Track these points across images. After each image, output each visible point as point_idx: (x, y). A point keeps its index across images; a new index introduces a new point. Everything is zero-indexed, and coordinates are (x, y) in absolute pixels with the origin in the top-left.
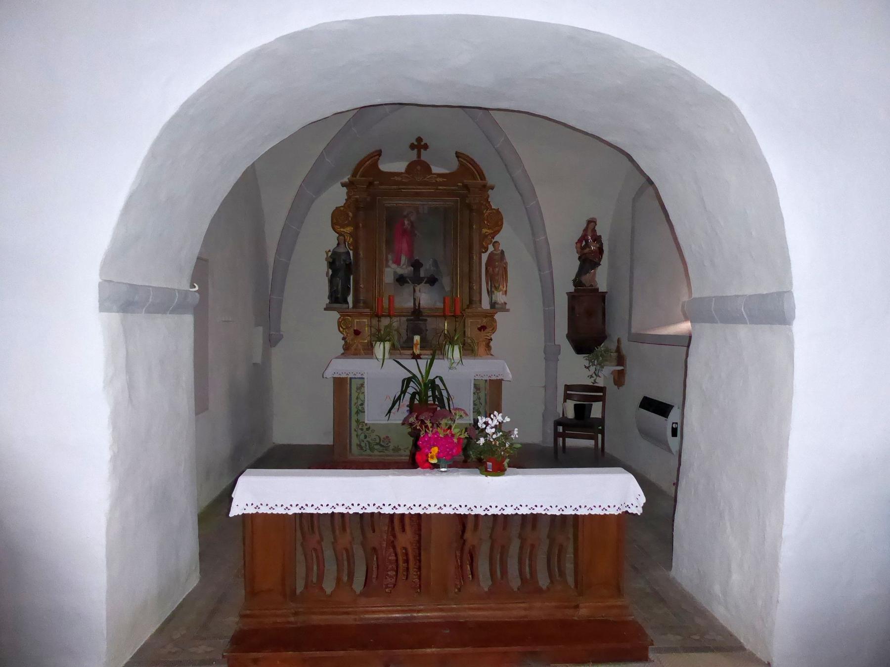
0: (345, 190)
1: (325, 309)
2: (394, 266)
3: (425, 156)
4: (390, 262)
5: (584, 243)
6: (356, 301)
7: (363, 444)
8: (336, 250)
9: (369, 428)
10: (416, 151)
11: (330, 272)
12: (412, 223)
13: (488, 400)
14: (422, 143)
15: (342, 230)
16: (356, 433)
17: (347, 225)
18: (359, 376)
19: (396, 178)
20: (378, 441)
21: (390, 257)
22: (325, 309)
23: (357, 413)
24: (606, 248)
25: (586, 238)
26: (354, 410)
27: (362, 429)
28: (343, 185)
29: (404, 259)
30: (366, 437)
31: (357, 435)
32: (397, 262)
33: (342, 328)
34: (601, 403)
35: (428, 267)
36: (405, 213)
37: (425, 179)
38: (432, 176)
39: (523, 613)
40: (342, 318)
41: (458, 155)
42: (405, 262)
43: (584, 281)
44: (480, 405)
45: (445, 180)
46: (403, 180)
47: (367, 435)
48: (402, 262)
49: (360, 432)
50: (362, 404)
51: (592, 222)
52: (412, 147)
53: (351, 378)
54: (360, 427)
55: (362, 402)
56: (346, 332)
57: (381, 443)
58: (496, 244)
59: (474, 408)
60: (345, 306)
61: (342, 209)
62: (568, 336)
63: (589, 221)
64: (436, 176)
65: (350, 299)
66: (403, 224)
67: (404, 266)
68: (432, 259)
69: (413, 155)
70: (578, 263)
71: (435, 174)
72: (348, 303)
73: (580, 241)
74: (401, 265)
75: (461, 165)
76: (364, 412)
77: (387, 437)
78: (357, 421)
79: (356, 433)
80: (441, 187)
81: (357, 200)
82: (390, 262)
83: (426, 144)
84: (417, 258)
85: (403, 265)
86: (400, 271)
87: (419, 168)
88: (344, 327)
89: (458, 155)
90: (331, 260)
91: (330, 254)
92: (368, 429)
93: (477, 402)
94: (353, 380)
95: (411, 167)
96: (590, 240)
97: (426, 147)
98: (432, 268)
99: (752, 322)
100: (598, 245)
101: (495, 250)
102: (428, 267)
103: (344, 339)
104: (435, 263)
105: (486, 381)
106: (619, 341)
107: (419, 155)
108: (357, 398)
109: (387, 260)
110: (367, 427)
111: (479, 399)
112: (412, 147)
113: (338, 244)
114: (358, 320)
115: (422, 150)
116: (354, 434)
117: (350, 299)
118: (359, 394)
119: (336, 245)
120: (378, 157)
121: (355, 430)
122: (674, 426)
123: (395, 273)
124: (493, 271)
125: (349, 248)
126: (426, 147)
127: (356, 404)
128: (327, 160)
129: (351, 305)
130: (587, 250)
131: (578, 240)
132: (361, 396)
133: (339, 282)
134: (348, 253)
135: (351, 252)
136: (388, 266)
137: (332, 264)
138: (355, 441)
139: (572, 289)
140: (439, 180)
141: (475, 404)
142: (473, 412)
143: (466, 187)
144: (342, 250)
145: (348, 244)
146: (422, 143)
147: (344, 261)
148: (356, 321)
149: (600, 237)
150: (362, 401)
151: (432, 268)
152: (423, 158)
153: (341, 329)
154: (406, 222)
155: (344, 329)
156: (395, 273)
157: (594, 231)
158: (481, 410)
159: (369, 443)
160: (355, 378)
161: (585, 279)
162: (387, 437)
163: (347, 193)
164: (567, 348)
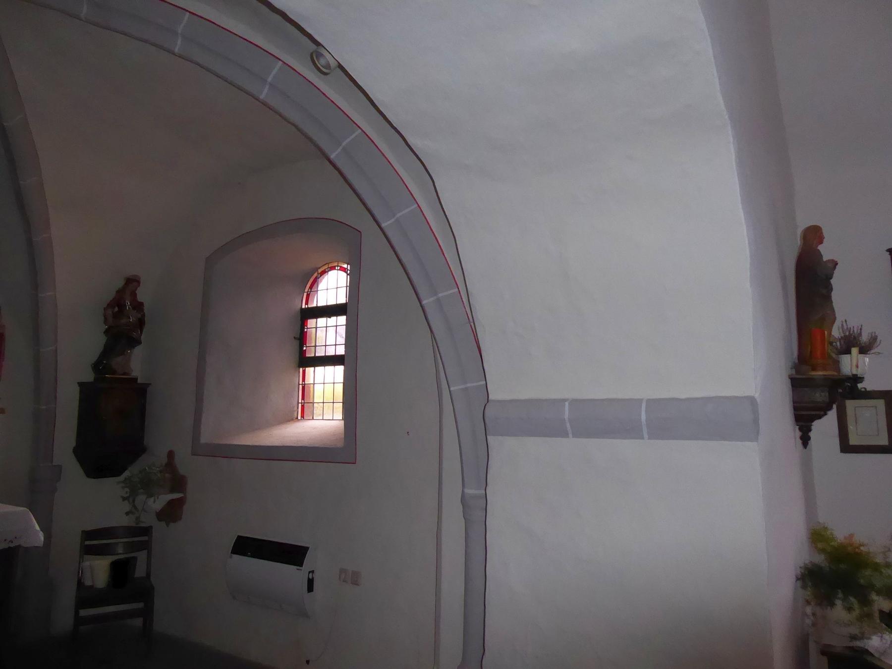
34: (145, 552)
51: (132, 282)
62: (77, 451)
70: (103, 339)
73: (110, 305)
99: (575, 435)
100: (139, 316)
106: (171, 455)
122: (311, 577)
130: (124, 321)
131: (108, 305)
149: (141, 304)
157: (134, 295)
161: (117, 362)
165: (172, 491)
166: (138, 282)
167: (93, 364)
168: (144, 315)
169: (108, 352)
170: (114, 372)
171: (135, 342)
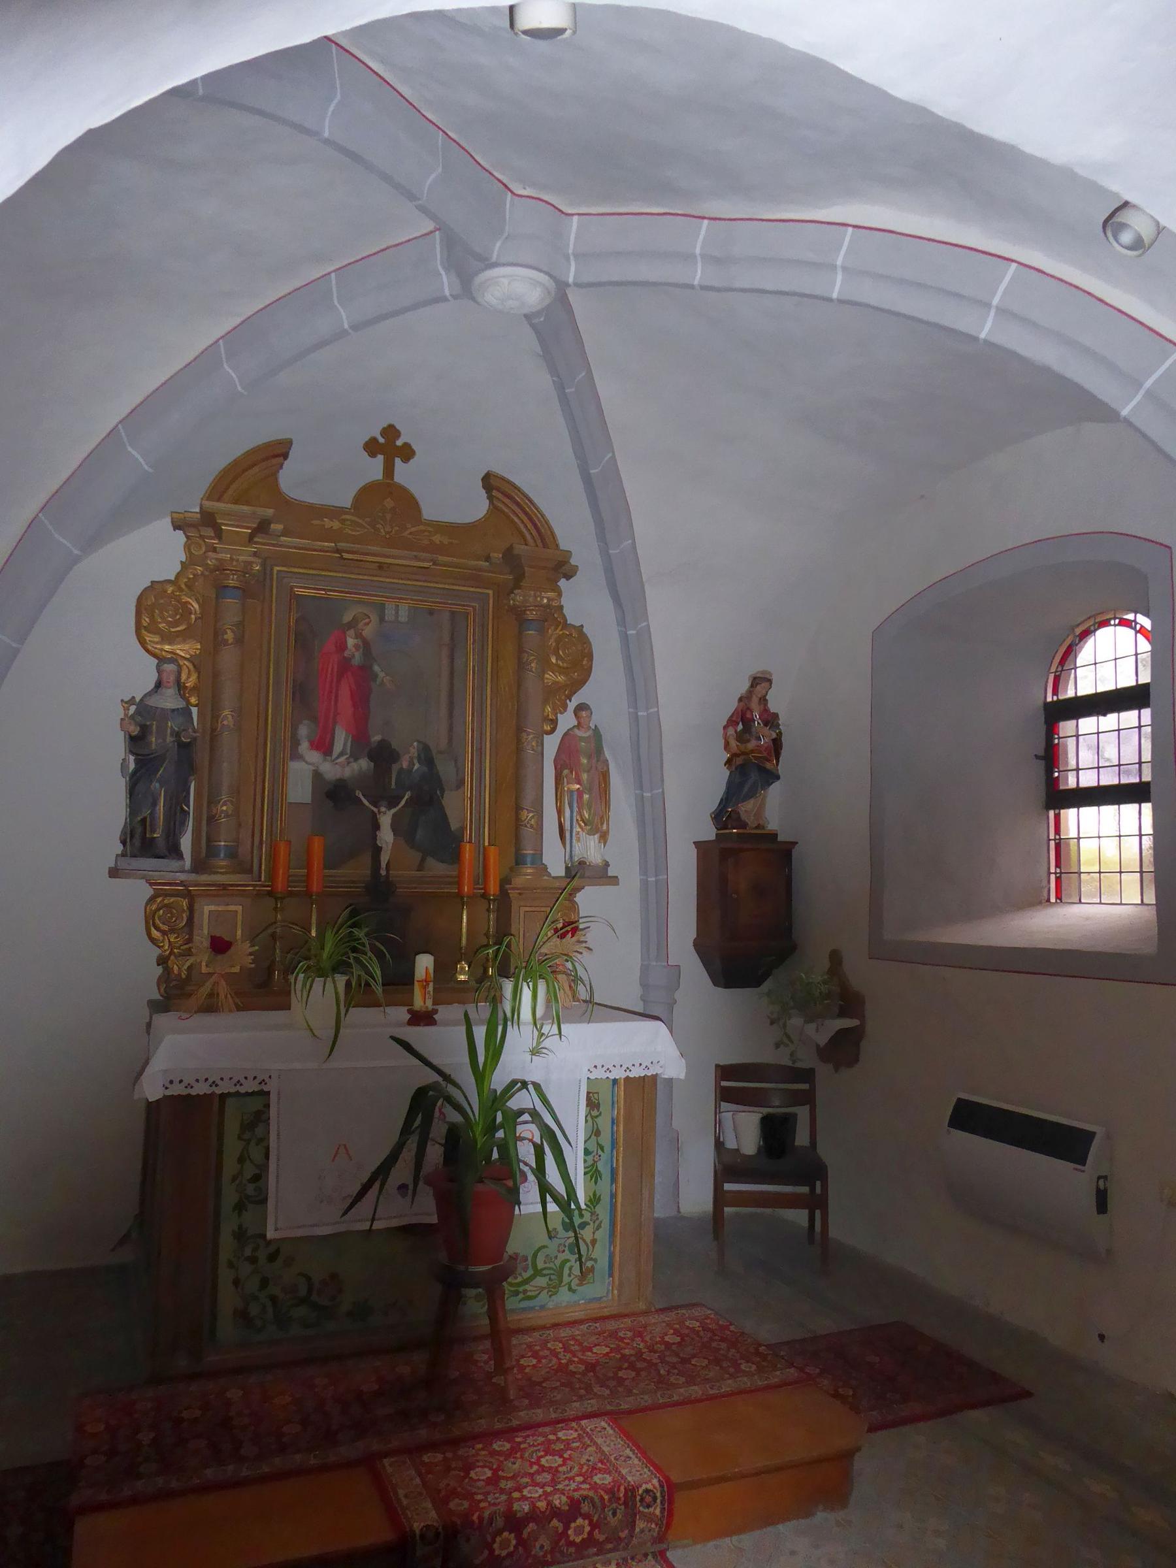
1: (114, 873)
2: (314, 757)
3: (403, 473)
7: (254, 1310)
8: (152, 702)
9: (278, 1251)
12: (366, 645)
14: (399, 443)
15: (167, 647)
17: (184, 636)
18: (250, 1087)
20: (303, 1292)
21: (303, 731)
23: (240, 1207)
25: (748, 716)
26: (230, 1196)
27: (253, 1260)
29: (341, 738)
30: (264, 1283)
31: (236, 1282)
32: (323, 745)
33: (158, 929)
34: (808, 1107)
36: (347, 618)
38: (422, 527)
42: (345, 745)
44: (600, 1152)
46: (347, 531)
48: (338, 747)
50: (256, 1178)
51: (760, 681)
52: (372, 447)
53: (223, 1097)
54: (248, 1252)
55: (257, 1172)
57: (314, 1297)
58: (584, 714)
59: (585, 1161)
63: (755, 678)
65: (186, 843)
66: (342, 647)
68: (419, 742)
69: (374, 469)
70: (726, 773)
71: (430, 523)
72: (180, 856)
73: (731, 722)
74: (334, 757)
75: (494, 508)
76: (264, 1201)
77: (334, 1276)
78: (240, 1235)
81: (221, 568)
82: (304, 746)
83: (407, 446)
85: (341, 754)
86: (332, 770)
87: (389, 503)
88: (165, 928)
89: (490, 482)
90: (135, 730)
91: (133, 709)
92: (272, 1258)
93: (592, 1147)
94: (230, 1103)
95: (369, 495)
97: (407, 453)
98: (417, 766)
100: (774, 736)
101: (579, 726)
102: (405, 765)
104: (427, 757)
105: (615, 1081)
106: (836, 958)
107: (389, 470)
108: (241, 1160)
109: (296, 743)
111: (597, 1133)
112: (372, 447)
113: (159, 685)
114: (213, 908)
115: (398, 461)
116: (225, 1276)
119: (151, 686)
121: (231, 1265)
122: (1102, 1186)
123: (317, 775)
126: (407, 453)
127: (234, 1179)
128: (130, 449)
130: (752, 745)
132: (256, 1153)
136: (296, 756)
137: (136, 742)
138: (228, 1299)
139: (709, 833)
140: (437, 539)
141: (587, 1152)
142: (585, 1174)
144: (169, 700)
146: (399, 443)
147: (177, 735)
149: (776, 716)
151: (417, 766)
153: (155, 933)
154: (351, 642)
155: (164, 933)
156: (317, 775)
157: (763, 700)
159: (273, 1299)
160: (237, 1094)
161: (746, 808)
162: (334, 1276)
163: (187, 547)
165: (843, 1013)
166: (770, 681)
167: (713, 813)
168: (780, 734)
170: (744, 825)
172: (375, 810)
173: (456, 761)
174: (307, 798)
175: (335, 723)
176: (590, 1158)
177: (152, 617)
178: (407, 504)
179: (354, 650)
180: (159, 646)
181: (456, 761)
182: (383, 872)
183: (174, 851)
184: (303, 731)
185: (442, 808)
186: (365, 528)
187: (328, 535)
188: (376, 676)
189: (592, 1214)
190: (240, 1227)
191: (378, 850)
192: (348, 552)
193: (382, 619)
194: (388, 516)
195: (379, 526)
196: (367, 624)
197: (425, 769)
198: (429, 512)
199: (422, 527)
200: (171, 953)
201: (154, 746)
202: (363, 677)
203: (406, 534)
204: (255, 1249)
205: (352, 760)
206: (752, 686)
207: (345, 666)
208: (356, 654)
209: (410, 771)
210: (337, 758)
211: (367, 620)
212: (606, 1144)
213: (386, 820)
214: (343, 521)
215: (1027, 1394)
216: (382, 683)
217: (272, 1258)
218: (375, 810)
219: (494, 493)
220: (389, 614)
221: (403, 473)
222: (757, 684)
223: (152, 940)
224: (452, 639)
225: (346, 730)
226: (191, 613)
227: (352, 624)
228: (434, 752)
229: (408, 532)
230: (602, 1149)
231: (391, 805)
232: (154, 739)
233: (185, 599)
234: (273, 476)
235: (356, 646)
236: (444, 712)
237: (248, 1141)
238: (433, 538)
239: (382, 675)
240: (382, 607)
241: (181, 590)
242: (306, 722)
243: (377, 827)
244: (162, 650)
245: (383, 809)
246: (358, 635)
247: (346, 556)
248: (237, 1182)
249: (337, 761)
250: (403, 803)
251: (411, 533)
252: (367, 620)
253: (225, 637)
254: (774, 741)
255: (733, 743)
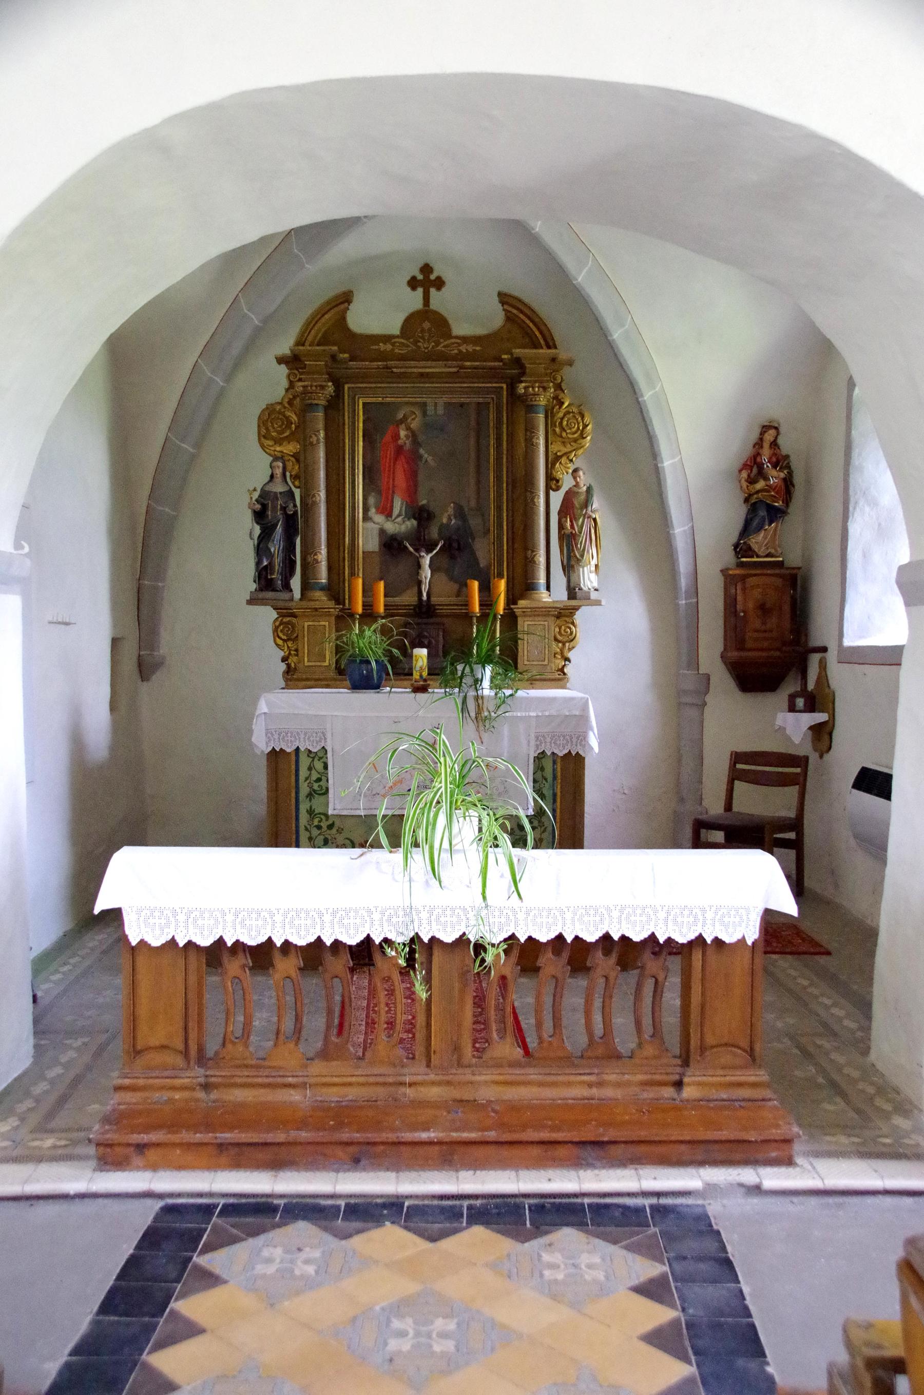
0: (283, 370)
1: (251, 602)
2: (379, 518)
3: (438, 300)
4: (373, 511)
5: (755, 470)
6: (306, 586)
8: (267, 488)
9: (333, 823)
10: (420, 291)
11: (257, 530)
12: (413, 435)
13: (559, 769)
14: (433, 277)
15: (278, 449)
16: (308, 834)
17: (288, 439)
19: (382, 346)
22: (251, 602)
23: (310, 796)
24: (798, 479)
25: (758, 460)
26: (304, 789)
27: (319, 827)
28: (280, 360)
29: (398, 505)
33: (281, 638)
35: (445, 521)
36: (400, 416)
37: (439, 348)
38: (453, 340)
39: (585, 1092)
40: (280, 619)
41: (505, 299)
43: (755, 547)
44: (544, 782)
45: (478, 348)
46: (397, 351)
47: (329, 838)
48: (396, 511)
49: (315, 832)
52: (413, 283)
54: (316, 822)
55: (320, 776)
56: (288, 647)
60: (285, 595)
61: (278, 408)
63: (764, 427)
64: (459, 341)
65: (296, 583)
66: (396, 437)
67: (400, 519)
68: (454, 503)
69: (414, 300)
71: (457, 337)
73: (745, 466)
74: (393, 517)
75: (509, 318)
78: (311, 812)
79: (308, 834)
80: (468, 364)
82: (372, 512)
83: (439, 278)
84: (424, 502)
85: (399, 516)
86: (391, 527)
87: (427, 325)
88: (285, 638)
89: (505, 299)
91: (256, 495)
92: (330, 827)
96: (767, 466)
97: (439, 283)
98: (453, 522)
100: (782, 475)
102: (445, 521)
103: (284, 659)
104: (460, 513)
108: (310, 769)
110: (330, 822)
111: (542, 769)
112: (413, 283)
113: (272, 476)
114: (311, 623)
115: (433, 291)
117: (296, 583)
118: (313, 761)
120: (346, 304)
121: (306, 829)
123: (382, 532)
124: (572, 526)
125: (293, 483)
126: (439, 283)
127: (307, 779)
129: (297, 594)
130: (761, 484)
133: (276, 546)
134: (291, 494)
135: (297, 493)
137: (259, 516)
140: (463, 348)
143: (518, 362)
144: (278, 487)
145: (291, 476)
146: (433, 277)
147: (284, 509)
148: (306, 624)
149: (787, 457)
150: (319, 773)
152: (435, 304)
153: (280, 642)
154: (403, 433)
156: (382, 532)
157: (774, 444)
158: (545, 791)
161: (757, 541)
164: (722, 679)
165: (811, 706)
168: (790, 474)
169: (746, 530)
171: (776, 514)
172: (417, 554)
173: (483, 515)
174: (377, 549)
175: (393, 492)
176: (537, 785)
177: (267, 429)
178: (441, 324)
179: (405, 439)
180: (272, 448)
181: (483, 515)
182: (425, 597)
183: (287, 587)
184: (371, 501)
185: (473, 553)
186: (408, 346)
187: (383, 356)
188: (421, 457)
189: (539, 822)
190: (311, 807)
191: (419, 583)
192: (396, 367)
193: (425, 414)
194: (426, 335)
195: (419, 344)
196: (413, 419)
197: (460, 523)
198: (460, 329)
199: (453, 340)
200: (290, 654)
201: (270, 517)
202: (414, 458)
203: (439, 348)
204: (320, 822)
205: (406, 519)
206: (761, 434)
207: (399, 450)
208: (407, 442)
209: (448, 525)
210: (396, 518)
211: (413, 416)
212: (550, 777)
213: (426, 560)
214: (393, 344)
215: (828, 953)
216: (426, 461)
217: (330, 827)
218: (417, 554)
219: (506, 307)
220: (430, 410)
221: (438, 300)
222: (765, 432)
223: (277, 645)
224: (478, 424)
225: (402, 499)
226: (292, 423)
227: (402, 421)
228: (466, 509)
229: (442, 345)
230: (546, 780)
231: (429, 551)
232: (270, 513)
233: (288, 414)
234: (343, 319)
235: (407, 436)
236: (472, 481)
237: (313, 758)
238: (461, 348)
239: (426, 456)
240: (424, 405)
241: (285, 408)
242: (373, 494)
243: (419, 566)
244: (275, 451)
245: (423, 554)
246: (408, 428)
247: (395, 370)
248: (308, 781)
249: (396, 520)
250: (438, 548)
251: (444, 347)
252: (413, 416)
253: (311, 440)
254: (785, 480)
255: (745, 484)
